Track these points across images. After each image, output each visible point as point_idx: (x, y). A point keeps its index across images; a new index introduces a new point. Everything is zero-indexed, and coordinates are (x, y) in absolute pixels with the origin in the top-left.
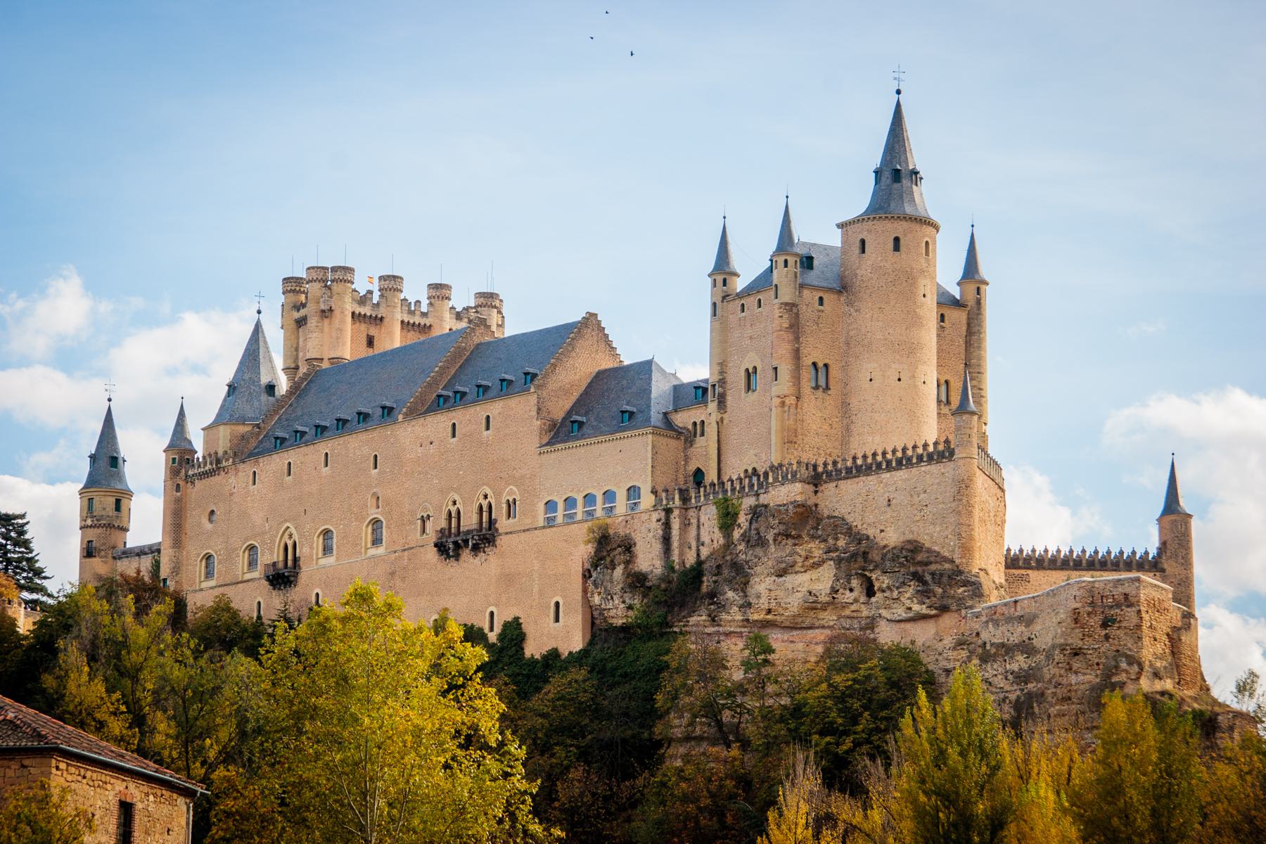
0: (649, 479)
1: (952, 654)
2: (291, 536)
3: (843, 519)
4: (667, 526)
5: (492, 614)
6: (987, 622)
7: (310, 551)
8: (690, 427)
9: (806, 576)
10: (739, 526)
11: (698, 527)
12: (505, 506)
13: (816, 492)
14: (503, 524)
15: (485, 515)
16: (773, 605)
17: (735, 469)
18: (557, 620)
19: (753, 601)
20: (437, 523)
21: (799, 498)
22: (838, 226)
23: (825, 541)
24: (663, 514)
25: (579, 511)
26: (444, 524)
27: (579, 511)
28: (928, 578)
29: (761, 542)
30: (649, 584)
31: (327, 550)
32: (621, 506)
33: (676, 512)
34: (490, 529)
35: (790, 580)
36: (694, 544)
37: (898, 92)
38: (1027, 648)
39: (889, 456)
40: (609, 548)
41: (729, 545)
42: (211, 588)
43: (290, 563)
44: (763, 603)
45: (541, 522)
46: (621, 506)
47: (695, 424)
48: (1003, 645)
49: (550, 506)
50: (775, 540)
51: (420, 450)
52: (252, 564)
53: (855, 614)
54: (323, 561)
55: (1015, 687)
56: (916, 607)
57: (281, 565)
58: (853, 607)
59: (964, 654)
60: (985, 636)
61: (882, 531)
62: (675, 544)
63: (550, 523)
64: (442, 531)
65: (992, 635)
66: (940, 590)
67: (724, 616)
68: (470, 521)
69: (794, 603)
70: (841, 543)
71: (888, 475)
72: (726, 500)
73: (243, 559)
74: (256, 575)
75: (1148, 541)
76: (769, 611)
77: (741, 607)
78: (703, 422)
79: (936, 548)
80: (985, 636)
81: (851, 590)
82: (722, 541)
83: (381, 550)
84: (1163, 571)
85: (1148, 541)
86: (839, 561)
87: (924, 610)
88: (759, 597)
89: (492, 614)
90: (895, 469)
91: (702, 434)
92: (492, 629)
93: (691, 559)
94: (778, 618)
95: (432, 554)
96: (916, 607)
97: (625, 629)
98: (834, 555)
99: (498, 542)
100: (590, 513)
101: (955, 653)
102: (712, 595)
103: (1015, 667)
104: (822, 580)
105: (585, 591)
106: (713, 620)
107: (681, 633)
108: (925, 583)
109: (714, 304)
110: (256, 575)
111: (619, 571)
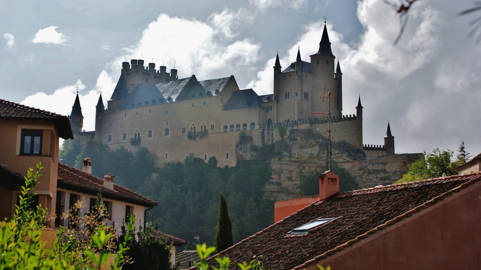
0: (258, 120)
1: (358, 172)
2: (137, 131)
3: (321, 134)
4: (263, 134)
5: (206, 155)
6: (370, 164)
7: (144, 136)
8: (267, 107)
9: (310, 150)
10: (286, 135)
11: (272, 135)
12: (210, 126)
13: (312, 127)
14: (210, 131)
15: (203, 128)
16: (299, 157)
17: (282, 119)
18: (227, 157)
19: (292, 155)
21: (308, 128)
22: (310, 56)
23: (316, 140)
24: (262, 130)
25: (235, 128)
26: (190, 130)
27: (235, 128)
28: (351, 151)
29: (295, 139)
30: (258, 149)
31: (150, 135)
32: (249, 128)
33: (266, 130)
34: (205, 132)
35: (305, 150)
36: (271, 139)
38: (385, 171)
39: (335, 118)
40: (245, 139)
41: (283, 140)
42: (111, 144)
43: (137, 139)
44: (296, 156)
45: (222, 131)
46: (249, 128)
47: (269, 107)
48: (375, 170)
49: (226, 127)
50: (301, 139)
52: (124, 138)
53: (324, 160)
54: (149, 139)
55: (380, 181)
56: (347, 159)
57: (134, 139)
58: (324, 158)
59: (362, 172)
60: (368, 167)
61: (333, 138)
62: (266, 138)
63: (225, 131)
64: (189, 132)
65: (371, 167)
66: (354, 155)
67: (283, 159)
68: (198, 130)
69: (306, 156)
70: (321, 141)
71: (335, 123)
72: (282, 127)
73: (121, 137)
74: (126, 141)
75: (381, 143)
76: (298, 158)
77: (289, 157)
78: (271, 106)
79: (351, 143)
80: (368, 167)
81: (324, 153)
82: (280, 139)
83: (168, 136)
84: (387, 151)
85: (381, 143)
86: (320, 146)
87: (350, 160)
88: (295, 154)
89: (206, 155)
90: (337, 121)
91: (271, 109)
92: (206, 159)
93: (270, 143)
94: (300, 160)
95: (186, 138)
96: (347, 159)
97: (248, 161)
98: (319, 144)
99: (208, 136)
100: (239, 130)
101: (359, 172)
102: (279, 153)
103: (380, 176)
104: (315, 151)
105: (236, 150)
106: (280, 160)
107: (268, 163)
108: (350, 153)
110: (126, 141)
111: (249, 145)
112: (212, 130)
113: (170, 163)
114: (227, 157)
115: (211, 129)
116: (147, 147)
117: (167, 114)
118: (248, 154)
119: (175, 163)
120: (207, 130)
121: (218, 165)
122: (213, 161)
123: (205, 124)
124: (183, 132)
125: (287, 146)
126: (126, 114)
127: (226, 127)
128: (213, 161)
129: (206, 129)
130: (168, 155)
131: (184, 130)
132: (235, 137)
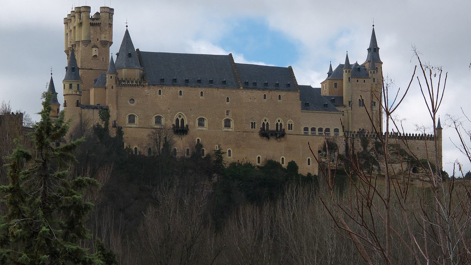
2: (180, 116)
5: (283, 158)
14: (287, 131)
18: (309, 164)
20: (258, 127)
25: (317, 132)
27: (317, 132)
32: (332, 133)
37: (373, 26)
46: (332, 133)
49: (306, 129)
51: (249, 100)
68: (272, 127)
70: (407, 157)
83: (230, 130)
89: (283, 158)
92: (283, 163)
95: (257, 135)
104: (405, 166)
109: (349, 78)
112: (290, 130)
113: (235, 163)
114: (309, 164)
115: (289, 129)
116: (198, 140)
117: (228, 101)
118: (335, 162)
119: (243, 163)
120: (284, 130)
121: (300, 171)
122: (293, 166)
123: (281, 122)
124: (252, 128)
125: (372, 157)
126: (160, 91)
127: (306, 129)
128: (293, 166)
129: (283, 127)
130: (231, 152)
131: (253, 125)
132: (318, 142)
